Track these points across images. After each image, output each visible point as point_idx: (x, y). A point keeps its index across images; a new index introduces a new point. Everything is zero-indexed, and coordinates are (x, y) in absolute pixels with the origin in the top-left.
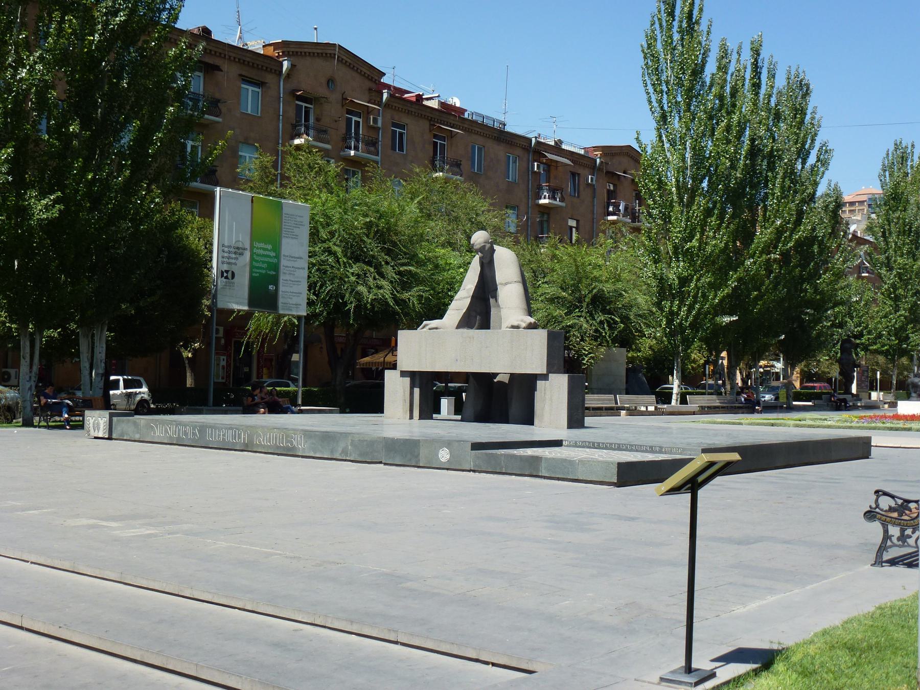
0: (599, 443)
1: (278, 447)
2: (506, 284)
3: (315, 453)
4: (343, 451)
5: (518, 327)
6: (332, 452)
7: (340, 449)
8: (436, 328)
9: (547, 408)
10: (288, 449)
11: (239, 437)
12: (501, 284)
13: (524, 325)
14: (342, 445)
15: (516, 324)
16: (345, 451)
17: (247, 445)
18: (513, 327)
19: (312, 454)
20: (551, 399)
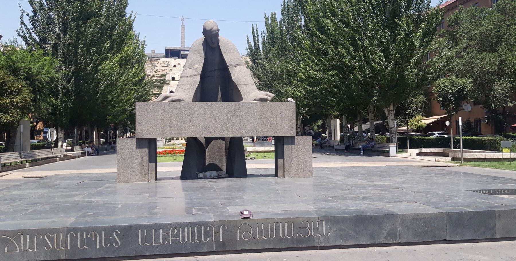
0: (494, 190)
1: (281, 240)
2: (236, 66)
3: (346, 241)
4: (389, 234)
5: (266, 100)
6: (372, 237)
7: (385, 233)
8: (179, 100)
9: (294, 162)
10: (299, 240)
11: (208, 234)
12: (231, 65)
13: (270, 98)
14: (387, 226)
15: (265, 97)
16: (392, 234)
17: (223, 243)
18: (261, 100)
19: (340, 242)
20: (298, 155)
